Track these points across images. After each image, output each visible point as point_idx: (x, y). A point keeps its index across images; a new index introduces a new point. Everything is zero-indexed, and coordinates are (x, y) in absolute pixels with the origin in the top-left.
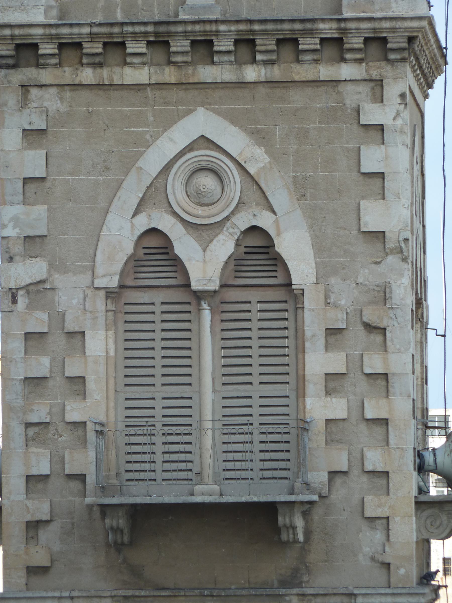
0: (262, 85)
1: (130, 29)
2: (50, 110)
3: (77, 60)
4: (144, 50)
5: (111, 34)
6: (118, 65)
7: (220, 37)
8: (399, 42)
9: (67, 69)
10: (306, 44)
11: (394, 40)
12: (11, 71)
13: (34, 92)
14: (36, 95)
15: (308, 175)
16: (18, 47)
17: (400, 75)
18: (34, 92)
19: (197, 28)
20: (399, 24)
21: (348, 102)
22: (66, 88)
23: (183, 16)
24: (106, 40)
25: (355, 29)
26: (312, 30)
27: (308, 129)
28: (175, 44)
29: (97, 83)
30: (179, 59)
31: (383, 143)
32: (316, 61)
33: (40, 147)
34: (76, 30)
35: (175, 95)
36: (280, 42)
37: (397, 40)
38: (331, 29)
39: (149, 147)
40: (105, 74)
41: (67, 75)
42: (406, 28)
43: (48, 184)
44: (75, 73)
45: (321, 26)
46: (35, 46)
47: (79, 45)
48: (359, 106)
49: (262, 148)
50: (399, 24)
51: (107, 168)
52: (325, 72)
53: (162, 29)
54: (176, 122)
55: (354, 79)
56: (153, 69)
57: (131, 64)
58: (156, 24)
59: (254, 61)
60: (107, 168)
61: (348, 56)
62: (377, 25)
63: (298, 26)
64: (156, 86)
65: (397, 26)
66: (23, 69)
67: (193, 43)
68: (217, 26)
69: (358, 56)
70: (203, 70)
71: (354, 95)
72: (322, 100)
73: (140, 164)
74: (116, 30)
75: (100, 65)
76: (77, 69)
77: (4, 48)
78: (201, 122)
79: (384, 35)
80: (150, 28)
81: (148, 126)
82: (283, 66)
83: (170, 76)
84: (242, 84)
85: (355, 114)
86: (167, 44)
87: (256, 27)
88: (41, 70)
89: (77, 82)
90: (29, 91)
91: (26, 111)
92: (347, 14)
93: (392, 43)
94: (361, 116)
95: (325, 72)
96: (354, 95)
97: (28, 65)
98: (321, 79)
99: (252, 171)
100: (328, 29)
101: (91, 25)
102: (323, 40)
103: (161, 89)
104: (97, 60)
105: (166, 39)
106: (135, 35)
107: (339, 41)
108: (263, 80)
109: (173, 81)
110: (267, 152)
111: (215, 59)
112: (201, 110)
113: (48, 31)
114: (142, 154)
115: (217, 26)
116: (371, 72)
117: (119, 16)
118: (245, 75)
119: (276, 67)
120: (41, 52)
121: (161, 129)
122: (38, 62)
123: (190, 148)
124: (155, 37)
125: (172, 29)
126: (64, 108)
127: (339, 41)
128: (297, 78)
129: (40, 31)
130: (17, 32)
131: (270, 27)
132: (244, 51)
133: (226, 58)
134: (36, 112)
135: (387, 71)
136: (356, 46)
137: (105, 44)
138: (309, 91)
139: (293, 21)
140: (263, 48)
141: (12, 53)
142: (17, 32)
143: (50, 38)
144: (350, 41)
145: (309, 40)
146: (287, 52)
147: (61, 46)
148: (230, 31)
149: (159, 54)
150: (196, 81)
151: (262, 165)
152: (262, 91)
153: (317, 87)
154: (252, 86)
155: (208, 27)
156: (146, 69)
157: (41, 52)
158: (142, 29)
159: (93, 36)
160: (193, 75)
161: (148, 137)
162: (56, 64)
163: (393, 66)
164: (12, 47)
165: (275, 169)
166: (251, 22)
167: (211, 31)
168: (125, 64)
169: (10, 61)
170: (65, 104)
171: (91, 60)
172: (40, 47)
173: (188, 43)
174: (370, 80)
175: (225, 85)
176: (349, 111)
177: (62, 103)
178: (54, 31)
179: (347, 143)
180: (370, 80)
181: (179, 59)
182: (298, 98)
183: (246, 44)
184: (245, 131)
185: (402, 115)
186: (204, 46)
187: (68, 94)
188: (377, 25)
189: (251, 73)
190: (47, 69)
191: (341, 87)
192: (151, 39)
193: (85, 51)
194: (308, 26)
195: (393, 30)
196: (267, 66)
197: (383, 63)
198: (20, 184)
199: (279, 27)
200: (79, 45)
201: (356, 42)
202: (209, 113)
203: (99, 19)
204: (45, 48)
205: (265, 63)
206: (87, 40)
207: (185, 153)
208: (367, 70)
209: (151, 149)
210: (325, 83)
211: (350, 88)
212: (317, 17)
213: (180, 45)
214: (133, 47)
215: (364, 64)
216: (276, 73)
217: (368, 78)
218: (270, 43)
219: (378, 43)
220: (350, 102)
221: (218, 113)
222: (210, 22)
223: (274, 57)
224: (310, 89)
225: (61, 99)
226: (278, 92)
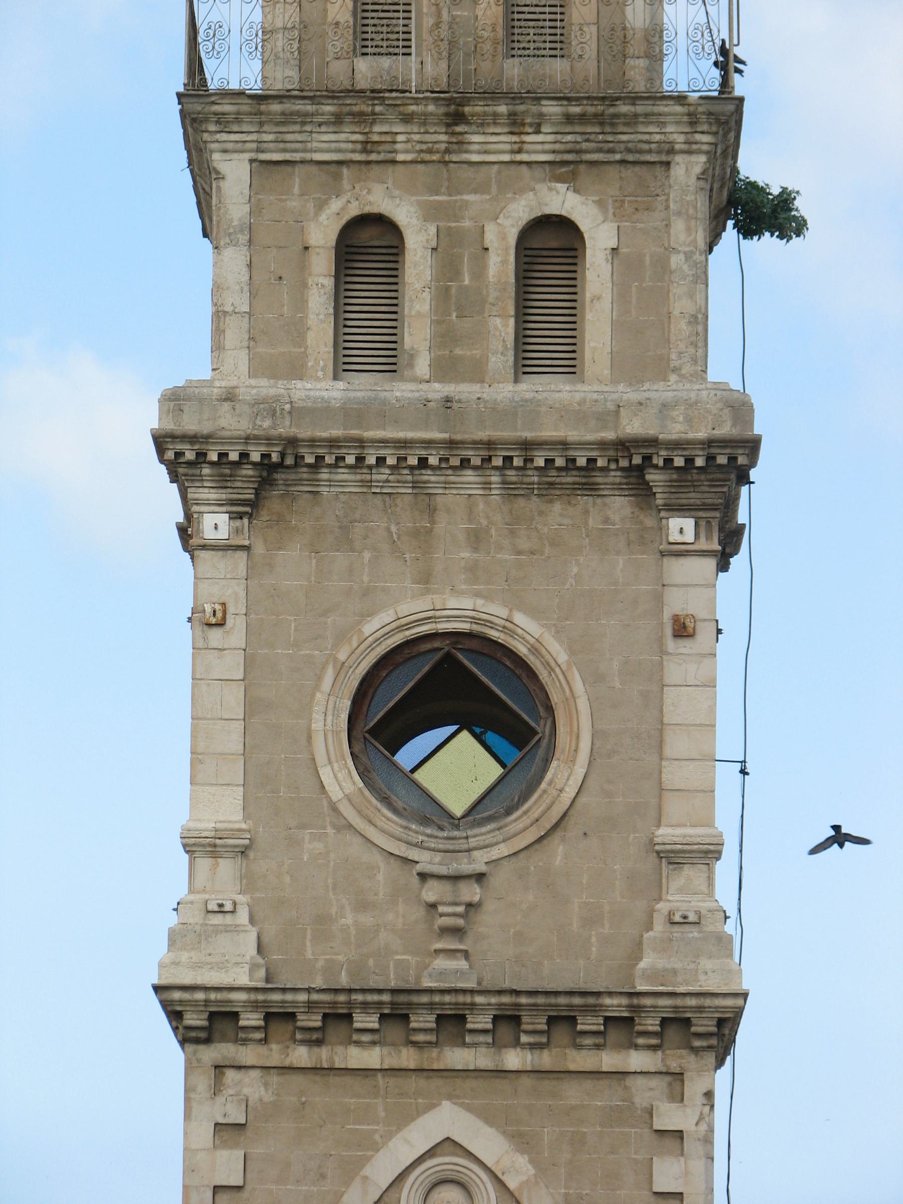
0: (526, 1075)
1: (359, 997)
2: (250, 1099)
3: (288, 1036)
4: (376, 1026)
5: (336, 1003)
6: (341, 1043)
7: (475, 1012)
8: (705, 1026)
9: (274, 1046)
10: (587, 1023)
11: (700, 1023)
12: (201, 1048)
13: (230, 1074)
14: (233, 1080)
15: (584, 1192)
16: (212, 1016)
17: (705, 1068)
18: (231, 1075)
19: (447, 998)
20: (708, 1002)
21: (637, 1100)
22: (272, 1071)
23: (427, 983)
24: (327, 1011)
25: (651, 1007)
26: (595, 1006)
27: (585, 1133)
28: (417, 1019)
29: (314, 1066)
30: (421, 1037)
31: (682, 1154)
32: (598, 1047)
33: (236, 1146)
34: (289, 997)
35: (414, 1085)
36: (551, 1021)
37: (705, 1023)
38: (619, 1006)
39: (378, 1150)
40: (323, 1056)
41: (274, 1054)
42: (716, 1007)
43: (245, 1194)
44: (285, 1051)
45: (608, 1001)
46: (235, 1016)
47: (292, 1016)
48: (652, 1106)
49: (526, 1156)
50: (708, 1002)
51: (323, 1176)
52: (608, 1060)
53: (402, 998)
54: (414, 1119)
55: (646, 1070)
56: (386, 1050)
57: (358, 1043)
58: (394, 991)
59: (517, 1043)
60: (323, 1176)
61: (641, 1041)
62: (679, 1002)
63: (577, 1001)
64: (389, 1072)
65: (706, 1005)
66: (218, 1045)
67: (440, 1018)
68: (472, 997)
69: (654, 1041)
70: (451, 1053)
71: (644, 1092)
72: (604, 1097)
73: (367, 1171)
74: (342, 998)
75: (319, 1043)
76: (288, 1047)
77: (195, 1016)
78: (447, 1119)
79: (688, 1015)
80: (386, 998)
81: (378, 1123)
82: (554, 1051)
83: (408, 1060)
84: (501, 1073)
85: (647, 1116)
86: (406, 1018)
87: (523, 1000)
88: (240, 1047)
89: (287, 1063)
90: (223, 1074)
91: (220, 1100)
92: (641, 988)
93: (697, 1025)
94: (654, 1119)
95: (608, 1060)
96: (644, 1092)
97: (224, 1039)
98: (604, 1069)
99: (512, 1184)
100: (615, 1005)
101: (309, 990)
102: (607, 1019)
103: (396, 1076)
104: (315, 1036)
105: (404, 1012)
106: (365, 1005)
107: (629, 1021)
108: (529, 1069)
109: (412, 1067)
110: (531, 1161)
111: (468, 1039)
112: (446, 1104)
113: (253, 996)
114: (368, 1159)
115: (472, 997)
116: (668, 1063)
117: (344, 981)
118: (505, 1061)
119: (546, 1053)
120: (242, 1023)
121: (394, 1128)
122: (240, 1036)
123: (431, 1153)
124: (392, 1009)
125: (415, 999)
126: (268, 1097)
127: (629, 1021)
128: (572, 1067)
129: (242, 996)
130: (213, 996)
131: (541, 1000)
132: (505, 1031)
133: (481, 1038)
134: (232, 1102)
135: (690, 1061)
136: (650, 1028)
137: (325, 1016)
138: (588, 1084)
139: (571, 993)
140: (530, 1027)
141: (205, 1023)
142: (213, 996)
143: (255, 1006)
144: (644, 1022)
145: (590, 1020)
146: (561, 1034)
147: (269, 1017)
148: (489, 1005)
149: (395, 1032)
150: (442, 1067)
151: (525, 1178)
152: (526, 1082)
153: (598, 1079)
154: (513, 1076)
155: (461, 999)
156: (377, 1051)
157: (242, 1023)
158: (375, 998)
159: (311, 1006)
160: (438, 1059)
161: (377, 1137)
162: (261, 1040)
163: (696, 1055)
164: (206, 1015)
165: (542, 1184)
166: (517, 993)
167: (465, 1004)
168: (351, 1042)
169: (203, 1035)
170: (270, 1091)
171: (307, 1036)
172: (242, 1016)
173: (433, 1018)
174: (667, 1073)
175: (478, 1072)
176: (639, 1112)
177: (266, 1090)
178: (261, 997)
179: (635, 1153)
180: (667, 1073)
181: (421, 1037)
182: (573, 1093)
183: (508, 1020)
184: (504, 1133)
185: (707, 1119)
186: (452, 1023)
187: (275, 1079)
188: (679, 1002)
189: (513, 1059)
190: (249, 1046)
191: (630, 1081)
192: (386, 1011)
193: (299, 1024)
194: (591, 1000)
195: (700, 1009)
196: (534, 1051)
197: (684, 1052)
198: (210, 1194)
199: (553, 1000)
200: (292, 1016)
201: (652, 1024)
202: (456, 1108)
203: (319, 983)
204: (248, 1019)
205: (532, 1046)
206: (302, 1010)
207: (425, 1161)
208: (663, 1060)
209: (381, 1152)
210: (609, 1075)
211: (640, 1081)
212: (602, 990)
213: (423, 1020)
214: (363, 1020)
215: (660, 1053)
216: (546, 1060)
217: (664, 1070)
218: (539, 1021)
219: (677, 1025)
220: (641, 1100)
221: (469, 1109)
222: (464, 991)
223: (544, 1040)
224: (589, 1081)
225: (266, 1085)
226: (547, 1084)
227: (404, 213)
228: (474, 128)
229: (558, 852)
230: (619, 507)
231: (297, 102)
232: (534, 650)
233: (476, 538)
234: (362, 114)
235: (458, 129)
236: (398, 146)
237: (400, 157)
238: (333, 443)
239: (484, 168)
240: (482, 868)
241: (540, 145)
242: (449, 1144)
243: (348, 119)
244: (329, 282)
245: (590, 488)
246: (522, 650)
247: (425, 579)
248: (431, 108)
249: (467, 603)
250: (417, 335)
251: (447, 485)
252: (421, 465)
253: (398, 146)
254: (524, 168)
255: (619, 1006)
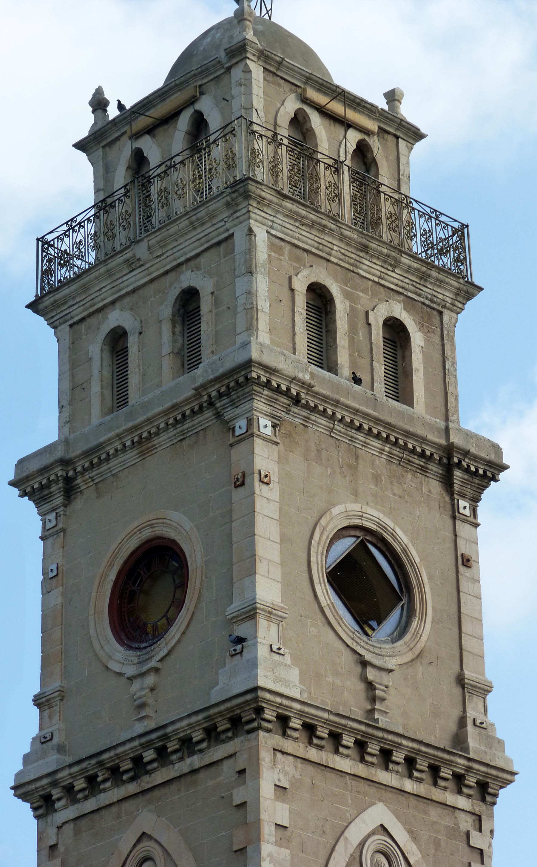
52: (451, 798)
72: (447, 821)
95: (451, 798)
151: (417, 859)
152: (413, 801)
182: (434, 813)
189: (409, 785)
191: (458, 814)
202: (385, 808)
211: (462, 815)
216: (422, 789)
226: (422, 805)
227: (335, 289)
228: (368, 257)
229: (420, 670)
230: (435, 486)
231: (300, 207)
232: (405, 551)
233: (377, 478)
234: (325, 226)
235: (361, 254)
236: (333, 252)
237: (332, 259)
238: (325, 399)
239: (366, 281)
240: (393, 667)
241: (395, 278)
242: (383, 828)
243: (317, 226)
244: (304, 312)
245: (424, 470)
246: (399, 550)
247: (355, 494)
248: (355, 236)
249: (376, 514)
250: (343, 357)
251: (365, 445)
252: (362, 427)
253: (333, 252)
254: (382, 289)
255: (463, 766)
